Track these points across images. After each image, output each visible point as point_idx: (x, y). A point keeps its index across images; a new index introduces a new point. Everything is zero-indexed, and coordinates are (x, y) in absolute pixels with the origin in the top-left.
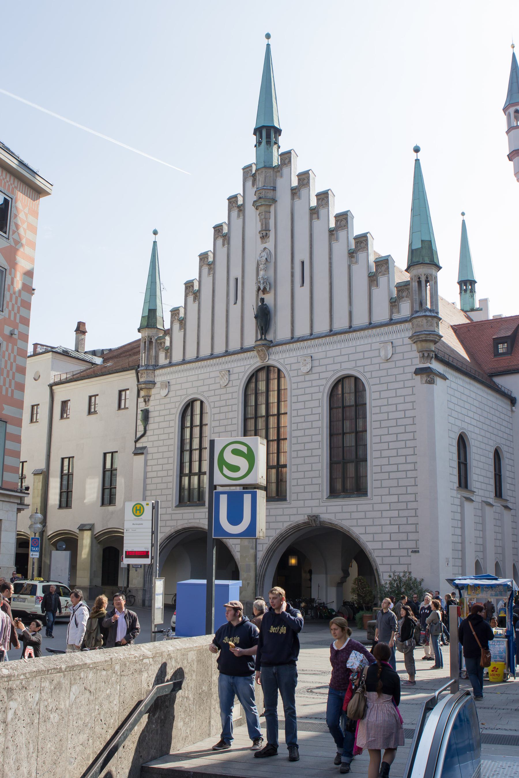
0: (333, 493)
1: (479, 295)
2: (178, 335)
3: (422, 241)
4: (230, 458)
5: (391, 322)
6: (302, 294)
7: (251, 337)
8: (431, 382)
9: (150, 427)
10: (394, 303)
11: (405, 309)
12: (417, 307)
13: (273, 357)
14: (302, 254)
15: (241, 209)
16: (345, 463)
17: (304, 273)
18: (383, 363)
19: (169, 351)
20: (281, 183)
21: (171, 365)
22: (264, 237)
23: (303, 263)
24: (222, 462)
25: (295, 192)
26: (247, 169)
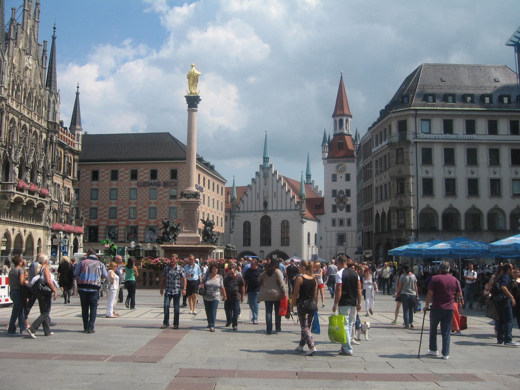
0: (282, 245)
2: (241, 206)
5: (295, 210)
6: (275, 200)
7: (262, 208)
9: (235, 226)
10: (296, 206)
11: (298, 207)
14: (275, 190)
15: (259, 176)
16: (284, 238)
17: (275, 195)
19: (239, 208)
20: (269, 172)
21: (240, 212)
22: (265, 185)
25: (273, 175)
26: (261, 166)
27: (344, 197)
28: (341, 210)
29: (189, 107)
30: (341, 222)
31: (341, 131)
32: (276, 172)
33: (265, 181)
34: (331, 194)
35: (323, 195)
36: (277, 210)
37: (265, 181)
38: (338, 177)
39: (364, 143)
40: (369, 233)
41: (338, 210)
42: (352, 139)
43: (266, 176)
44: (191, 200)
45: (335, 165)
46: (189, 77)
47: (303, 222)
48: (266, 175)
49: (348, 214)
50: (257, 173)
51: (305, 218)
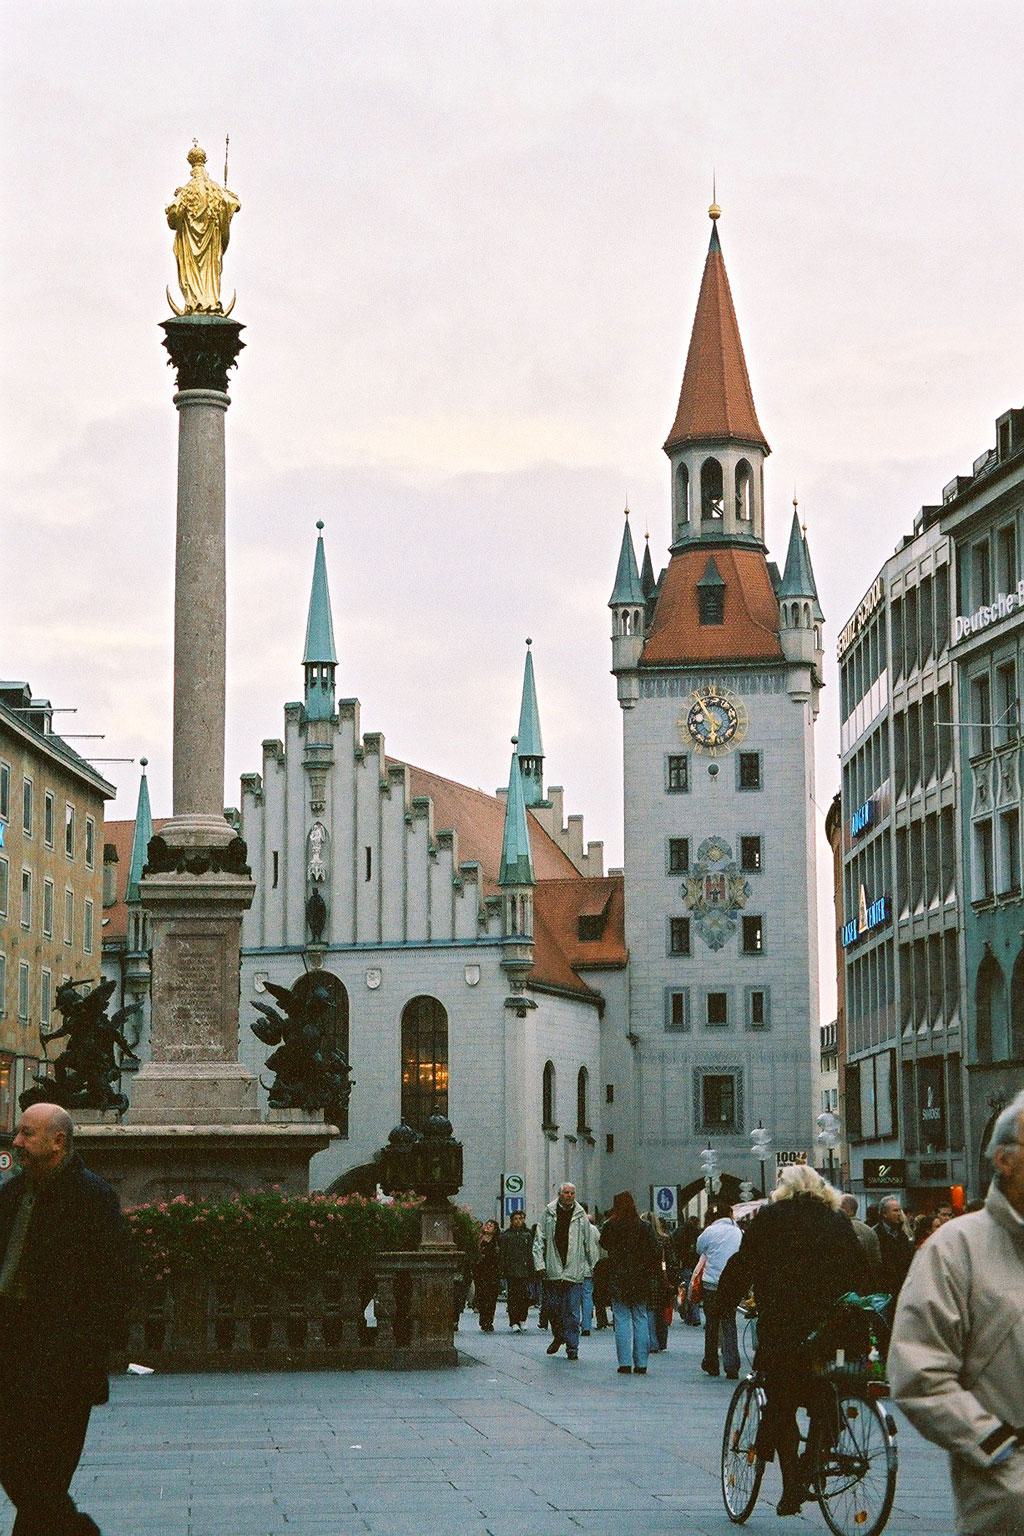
1: (549, 779)
3: (518, 856)
4: (511, 1183)
6: (367, 890)
7: (297, 936)
8: (523, 1015)
10: (482, 923)
11: (494, 929)
12: (509, 932)
13: (328, 964)
14: (367, 839)
15: (282, 763)
18: (470, 988)
22: (317, 810)
23: (369, 850)
24: (508, 1185)
26: (291, 710)
27: (729, 875)
28: (715, 944)
29: (183, 382)
30: (717, 1007)
31: (711, 527)
32: (374, 741)
33: (317, 788)
34: (662, 857)
35: (613, 860)
36: (379, 948)
37: (317, 788)
38: (697, 769)
39: (900, 590)
40: (932, 1066)
41: (697, 942)
42: (772, 567)
43: (317, 767)
44: (209, 878)
45: (683, 704)
46: (177, 220)
47: (520, 1008)
48: (324, 757)
49: (751, 963)
50: (270, 747)
51: (530, 988)
